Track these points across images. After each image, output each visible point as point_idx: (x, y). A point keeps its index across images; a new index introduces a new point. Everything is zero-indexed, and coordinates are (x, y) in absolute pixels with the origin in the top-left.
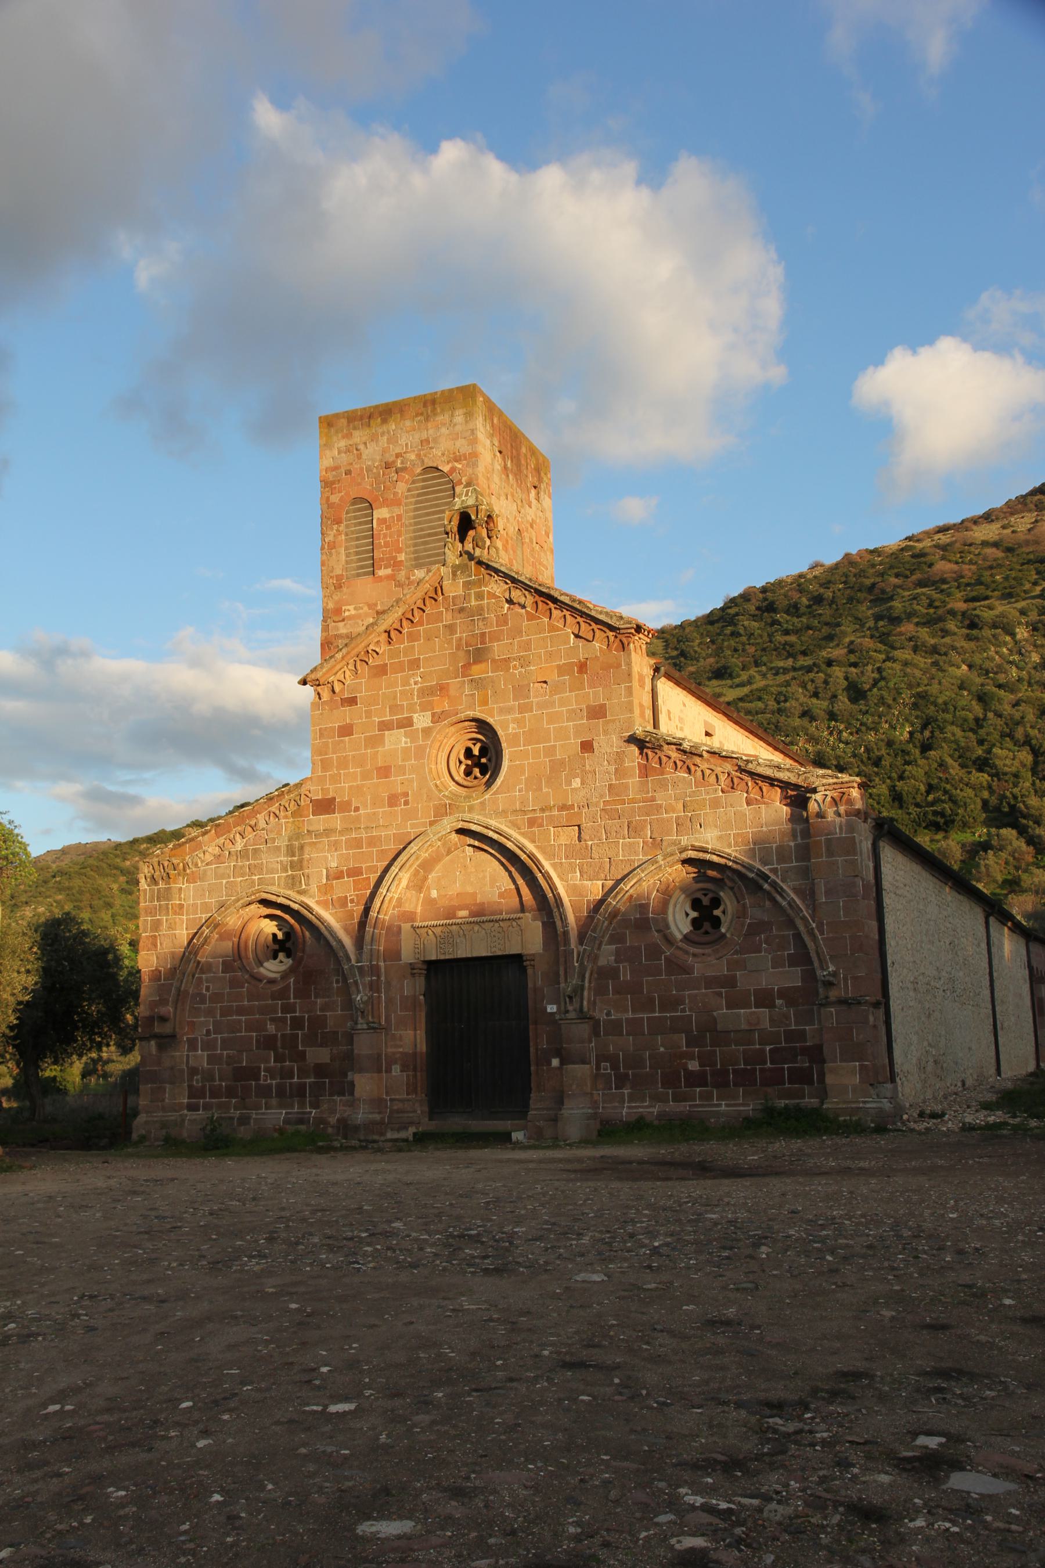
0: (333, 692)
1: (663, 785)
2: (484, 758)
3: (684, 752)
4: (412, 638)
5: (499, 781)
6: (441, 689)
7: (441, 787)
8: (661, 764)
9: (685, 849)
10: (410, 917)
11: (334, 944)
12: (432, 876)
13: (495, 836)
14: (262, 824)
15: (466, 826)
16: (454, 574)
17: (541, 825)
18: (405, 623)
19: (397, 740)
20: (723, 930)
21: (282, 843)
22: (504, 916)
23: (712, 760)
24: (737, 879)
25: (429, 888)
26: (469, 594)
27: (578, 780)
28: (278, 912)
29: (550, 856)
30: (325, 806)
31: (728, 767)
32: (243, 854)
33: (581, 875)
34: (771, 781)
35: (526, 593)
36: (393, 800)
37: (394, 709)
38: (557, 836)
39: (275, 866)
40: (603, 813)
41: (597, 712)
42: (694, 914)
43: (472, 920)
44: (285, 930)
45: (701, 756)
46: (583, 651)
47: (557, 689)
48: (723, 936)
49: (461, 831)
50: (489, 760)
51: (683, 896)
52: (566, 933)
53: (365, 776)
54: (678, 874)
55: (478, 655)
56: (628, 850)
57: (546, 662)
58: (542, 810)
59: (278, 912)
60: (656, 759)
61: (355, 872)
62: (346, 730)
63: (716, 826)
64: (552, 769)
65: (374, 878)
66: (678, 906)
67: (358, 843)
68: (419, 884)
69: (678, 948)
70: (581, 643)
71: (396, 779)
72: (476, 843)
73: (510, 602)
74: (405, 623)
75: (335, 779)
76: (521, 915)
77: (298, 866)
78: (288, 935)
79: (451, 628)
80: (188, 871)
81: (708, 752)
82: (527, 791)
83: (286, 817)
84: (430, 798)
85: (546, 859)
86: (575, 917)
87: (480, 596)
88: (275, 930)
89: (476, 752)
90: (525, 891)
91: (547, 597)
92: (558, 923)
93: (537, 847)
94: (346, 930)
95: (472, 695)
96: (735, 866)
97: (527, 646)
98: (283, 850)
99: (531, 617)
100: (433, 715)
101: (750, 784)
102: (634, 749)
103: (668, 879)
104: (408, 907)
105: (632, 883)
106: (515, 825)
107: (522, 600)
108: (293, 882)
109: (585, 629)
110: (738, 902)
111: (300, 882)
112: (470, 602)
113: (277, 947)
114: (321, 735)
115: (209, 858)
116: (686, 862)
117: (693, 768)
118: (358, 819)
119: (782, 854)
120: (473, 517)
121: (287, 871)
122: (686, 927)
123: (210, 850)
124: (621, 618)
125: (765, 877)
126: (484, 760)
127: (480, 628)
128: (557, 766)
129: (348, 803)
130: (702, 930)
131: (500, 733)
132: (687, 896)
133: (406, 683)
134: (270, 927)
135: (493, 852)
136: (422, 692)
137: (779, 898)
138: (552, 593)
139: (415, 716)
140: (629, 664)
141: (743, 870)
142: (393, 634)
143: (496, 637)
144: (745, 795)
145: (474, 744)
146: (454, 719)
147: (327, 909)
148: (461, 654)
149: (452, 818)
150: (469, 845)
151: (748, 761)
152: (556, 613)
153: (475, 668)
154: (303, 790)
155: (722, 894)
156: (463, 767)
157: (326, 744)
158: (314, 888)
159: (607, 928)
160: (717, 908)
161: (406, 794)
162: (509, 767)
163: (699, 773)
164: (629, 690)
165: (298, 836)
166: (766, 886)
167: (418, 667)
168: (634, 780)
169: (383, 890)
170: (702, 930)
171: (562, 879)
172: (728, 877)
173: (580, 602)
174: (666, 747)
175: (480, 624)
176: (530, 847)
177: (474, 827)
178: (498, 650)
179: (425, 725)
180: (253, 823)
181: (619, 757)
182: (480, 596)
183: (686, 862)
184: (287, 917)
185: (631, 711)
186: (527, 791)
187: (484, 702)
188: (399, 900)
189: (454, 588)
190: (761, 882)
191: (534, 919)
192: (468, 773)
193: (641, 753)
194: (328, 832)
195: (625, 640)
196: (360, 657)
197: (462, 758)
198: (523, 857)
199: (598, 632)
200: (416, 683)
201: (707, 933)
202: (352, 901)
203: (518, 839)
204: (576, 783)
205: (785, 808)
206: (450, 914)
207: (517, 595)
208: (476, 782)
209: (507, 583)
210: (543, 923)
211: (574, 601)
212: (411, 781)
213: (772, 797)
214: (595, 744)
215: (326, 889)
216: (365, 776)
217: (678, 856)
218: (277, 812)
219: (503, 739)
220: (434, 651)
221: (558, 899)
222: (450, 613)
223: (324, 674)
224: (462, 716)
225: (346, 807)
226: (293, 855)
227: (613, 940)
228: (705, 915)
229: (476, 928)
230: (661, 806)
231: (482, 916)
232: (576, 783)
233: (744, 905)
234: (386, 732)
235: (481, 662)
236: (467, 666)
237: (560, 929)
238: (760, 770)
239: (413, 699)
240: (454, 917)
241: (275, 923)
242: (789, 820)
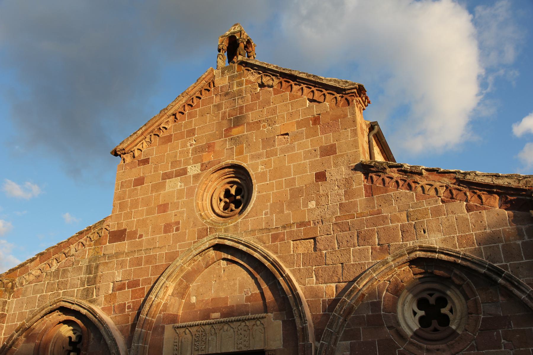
0: (134, 157)
1: (388, 201)
2: (239, 192)
3: (405, 172)
4: (191, 116)
5: (249, 208)
6: (209, 147)
7: (204, 216)
8: (384, 184)
9: (413, 250)
10: (173, 319)
11: (109, 342)
12: (193, 285)
13: (245, 249)
14: (73, 251)
15: (222, 241)
16: (223, 73)
17: (283, 240)
18: (187, 107)
19: (175, 185)
20: (454, 327)
21: (84, 264)
22: (250, 316)
23: (430, 177)
24: (463, 275)
25: (189, 295)
26: (233, 84)
27: (314, 203)
28: (73, 318)
29: (290, 264)
30: (118, 236)
31: (446, 180)
32: (56, 274)
33: (317, 279)
34: (489, 189)
35: (274, 77)
36: (167, 228)
37: (174, 163)
38: (296, 248)
39: (76, 282)
40: (335, 227)
41: (329, 151)
42: (421, 313)
43: (222, 320)
44: (78, 333)
45: (420, 174)
46: (316, 109)
47: (296, 137)
48: (454, 332)
49: (218, 247)
50: (243, 197)
51: (410, 296)
52: (304, 329)
53: (149, 212)
54: (406, 274)
55: (237, 121)
56: (360, 257)
57: (288, 120)
58: (284, 227)
59: (73, 318)
60: (380, 180)
61: (133, 284)
62: (140, 181)
63: (439, 231)
64: (292, 195)
65: (147, 288)
66: (406, 307)
67: (138, 262)
68: (182, 292)
69: (411, 343)
70: (314, 104)
71: (171, 212)
72: (229, 257)
73: (262, 85)
74: (187, 107)
75: (128, 216)
76: (264, 315)
77: (92, 281)
78: (80, 338)
79: (218, 107)
80: (15, 289)
81: (427, 170)
82: (272, 214)
83: (90, 245)
84: (195, 225)
85: (286, 267)
86: (312, 315)
87: (240, 84)
88: (71, 333)
89: (233, 191)
90: (268, 294)
91: (289, 78)
92: (298, 320)
93: (279, 257)
94: (121, 331)
95: (231, 149)
96: (464, 263)
97: (274, 111)
98: (84, 269)
99: (276, 92)
100: (202, 165)
101: (468, 194)
102: (360, 176)
103: (396, 280)
104: (172, 311)
105: (365, 282)
106: (260, 240)
107: (270, 83)
108: (87, 294)
109: (317, 95)
110: (467, 298)
111: (93, 294)
112: (233, 88)
113: (70, 348)
114: (122, 186)
115: (31, 278)
116: (413, 262)
117: (413, 185)
118: (140, 244)
119: (510, 252)
120: (237, 38)
121: (84, 285)
122: (416, 327)
123: (33, 273)
124: (347, 82)
125: (499, 272)
126: (238, 197)
127: (240, 102)
128: (296, 193)
129: (135, 232)
130: (432, 328)
131: (251, 172)
132: (415, 296)
133: (184, 145)
134: (66, 331)
135: (242, 263)
136: (195, 151)
137: (516, 291)
138: (293, 73)
139: (189, 167)
140: (354, 114)
141: (474, 267)
142: (178, 116)
143: (250, 108)
144: (465, 203)
145: (231, 187)
146: (217, 166)
147: (109, 314)
148: (225, 122)
149: (211, 236)
150: (224, 259)
151: (465, 174)
152: (296, 88)
153: (235, 131)
154: (104, 226)
155: (448, 293)
156: (223, 204)
157: (125, 192)
158: (102, 298)
159: (342, 325)
160: (444, 306)
161: (178, 223)
162: (258, 197)
163: (419, 189)
164: (355, 133)
165: (96, 258)
166: (500, 280)
167: (194, 134)
168: (361, 199)
169: (152, 296)
170: (432, 328)
171: (300, 283)
172: (456, 275)
173: (314, 76)
174: (388, 170)
175: (240, 101)
176: (274, 256)
177: (227, 243)
178: (251, 117)
179: (196, 173)
180: (66, 251)
181: (348, 182)
182: (240, 84)
183: (413, 262)
184: (79, 322)
185: (357, 147)
186: (272, 214)
187: (240, 152)
188: (166, 304)
189: (222, 82)
190: (494, 276)
191: (276, 318)
192: (226, 208)
193: (366, 178)
194: (117, 255)
195: (349, 98)
196: (154, 133)
197: (222, 197)
198: (267, 264)
199: (328, 96)
200: (191, 145)
201: (435, 330)
202: (129, 307)
203: (264, 249)
204: (312, 205)
205: (506, 212)
206: (206, 315)
207: (266, 80)
208: (232, 213)
209: (259, 73)
210: (284, 322)
211: (310, 76)
212: (183, 213)
213: (492, 203)
214: (327, 174)
215: (110, 298)
216: (149, 212)
217: (406, 257)
218: (84, 242)
219: (253, 177)
220: (205, 123)
221: (297, 297)
222: (218, 97)
223: (129, 145)
224: (223, 164)
225: (133, 235)
226: (91, 273)
227: (349, 335)
228: (433, 313)
229: (226, 327)
230: (386, 217)
232: (312, 205)
233: (476, 301)
234: (167, 180)
235: (238, 126)
236: (229, 130)
237: (299, 326)
238: (478, 180)
239: (188, 156)
240: (208, 317)
241: (71, 328)
242: (513, 221)
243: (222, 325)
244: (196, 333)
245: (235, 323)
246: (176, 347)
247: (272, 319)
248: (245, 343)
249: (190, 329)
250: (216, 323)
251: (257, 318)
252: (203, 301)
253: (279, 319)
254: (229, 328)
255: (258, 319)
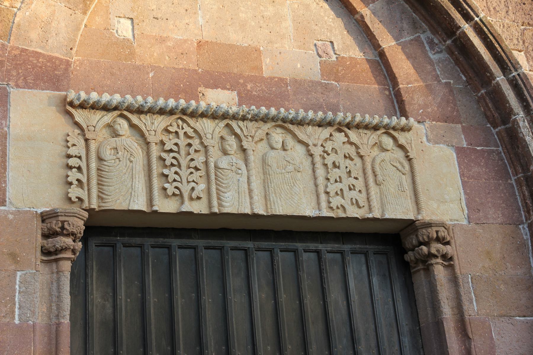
10: (48, 74)
210: (459, 151)
231: (275, 111)
243: (266, 127)
244: (165, 139)
245: (310, 129)
246: (74, 175)
247: (425, 139)
248: (354, 194)
249: (134, 119)
250: (244, 118)
251: (387, 127)
252: (162, 40)
253: (445, 142)
254: (290, 142)
255: (388, 130)
